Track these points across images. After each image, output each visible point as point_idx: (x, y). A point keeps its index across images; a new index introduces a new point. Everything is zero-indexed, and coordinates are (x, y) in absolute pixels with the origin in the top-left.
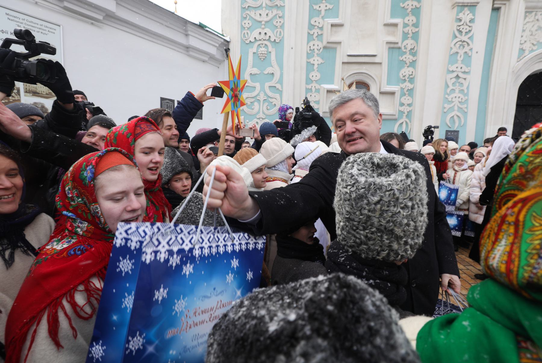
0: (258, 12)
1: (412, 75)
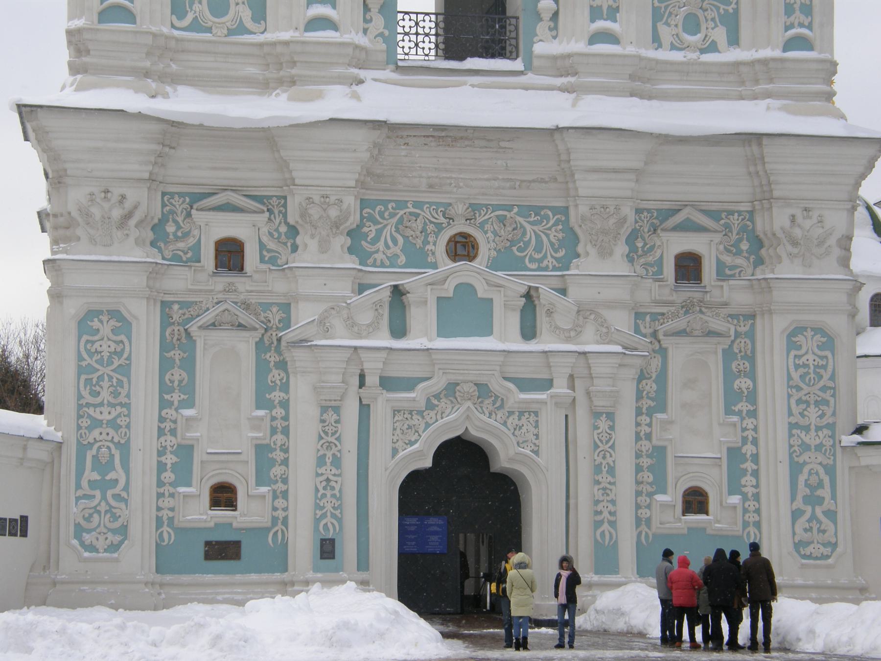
0: (98, 410)
1: (284, 474)
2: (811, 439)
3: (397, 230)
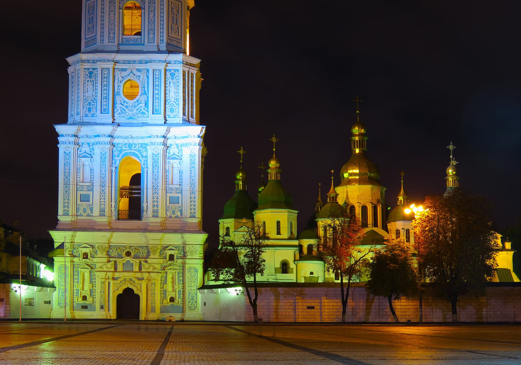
2: (193, 288)
3: (116, 251)
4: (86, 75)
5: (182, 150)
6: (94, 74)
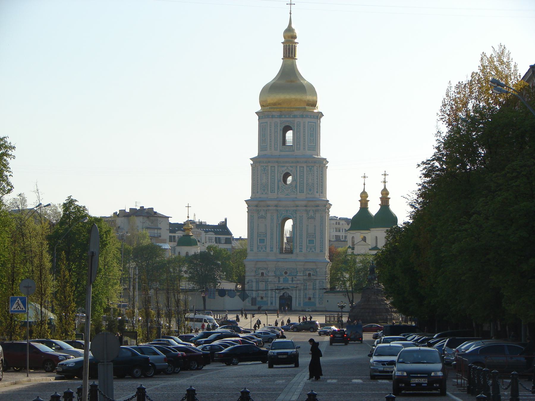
4: (262, 170)
5: (315, 213)
6: (266, 170)
